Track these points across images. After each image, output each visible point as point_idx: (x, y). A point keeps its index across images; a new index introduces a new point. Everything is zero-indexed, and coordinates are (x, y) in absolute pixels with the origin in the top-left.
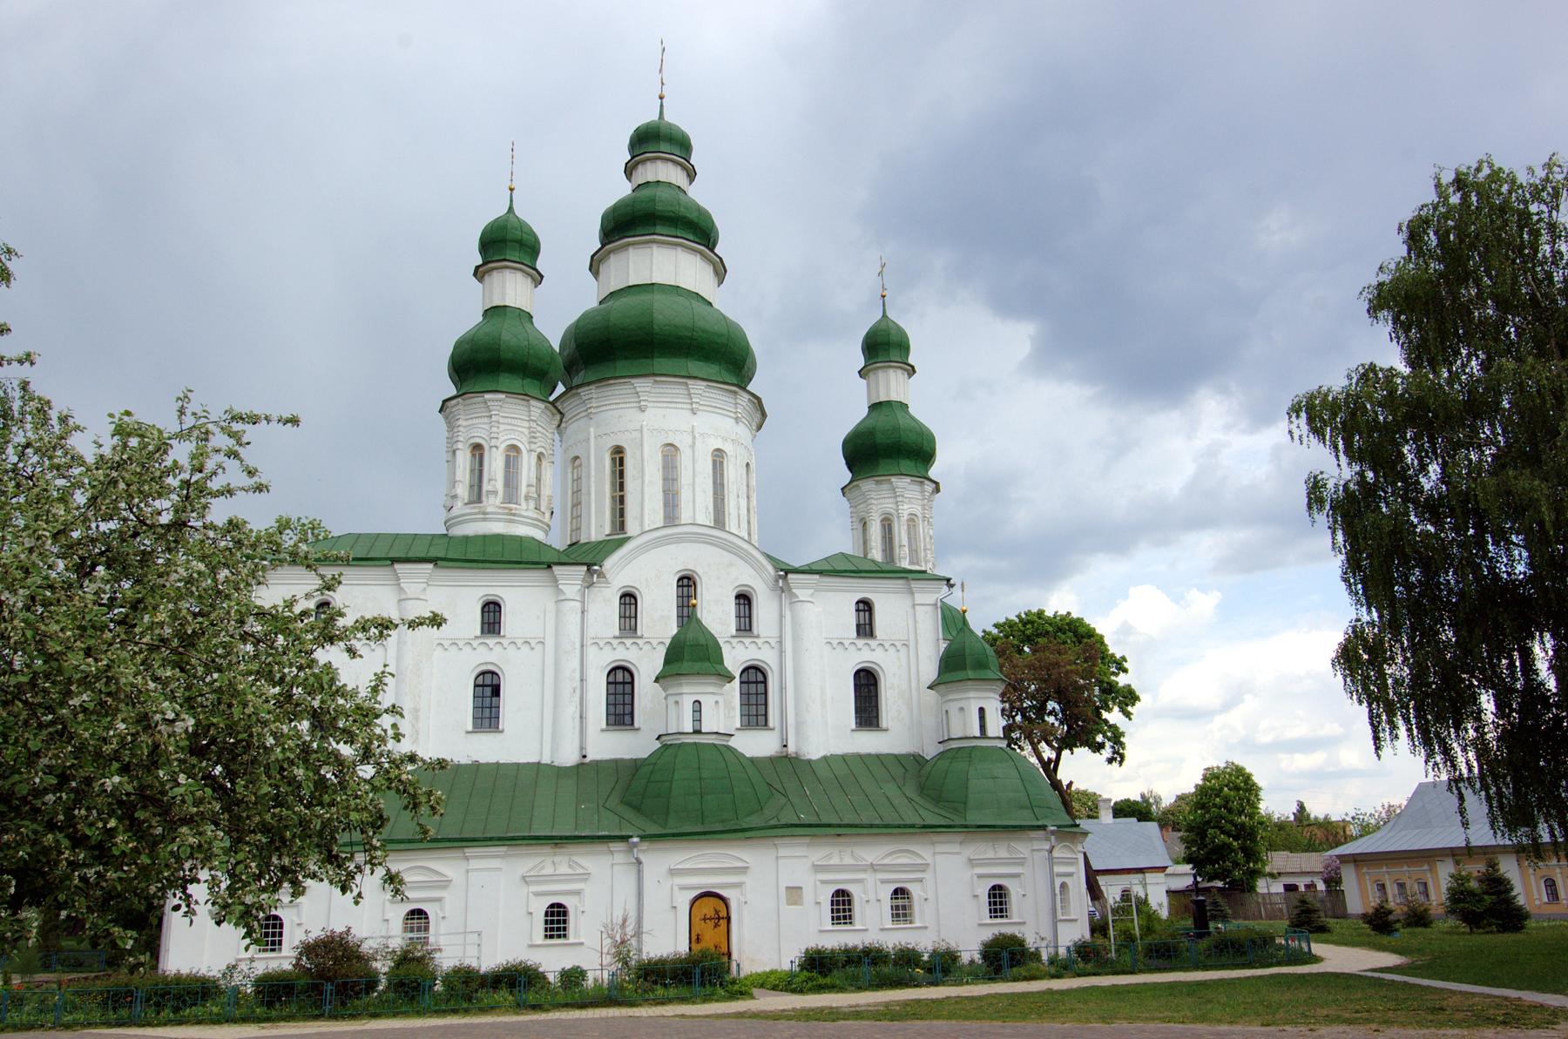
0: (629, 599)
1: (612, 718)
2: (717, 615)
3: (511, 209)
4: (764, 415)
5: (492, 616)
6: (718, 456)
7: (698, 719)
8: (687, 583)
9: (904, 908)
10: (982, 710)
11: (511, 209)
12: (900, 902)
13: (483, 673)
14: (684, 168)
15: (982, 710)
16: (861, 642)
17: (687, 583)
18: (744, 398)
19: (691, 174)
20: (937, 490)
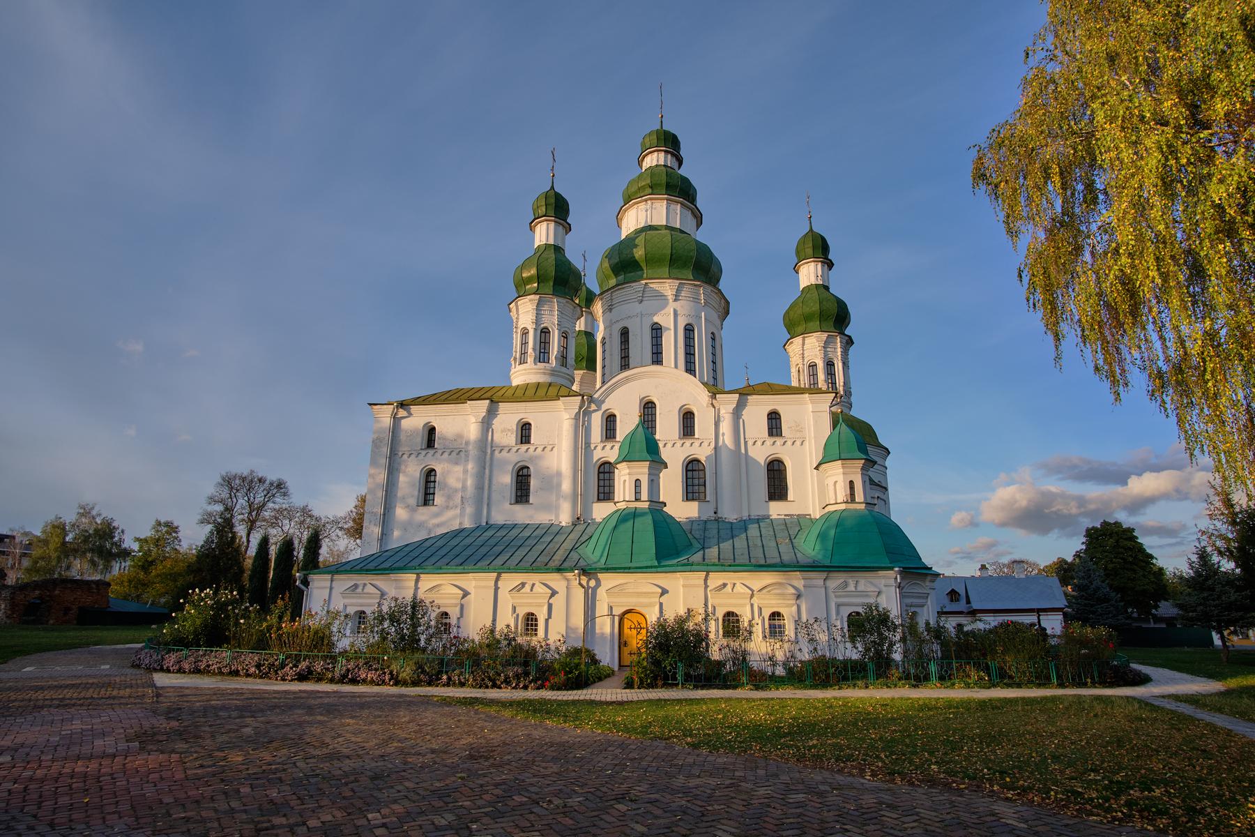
0: (610, 420)
1: (602, 496)
2: (667, 428)
3: (552, 187)
4: (728, 303)
5: (525, 432)
6: (689, 330)
7: (637, 492)
8: (648, 408)
9: (780, 626)
10: (851, 482)
11: (552, 187)
12: (777, 622)
13: (522, 468)
14: (673, 154)
15: (851, 482)
16: (769, 441)
17: (648, 408)
18: (709, 288)
19: (680, 162)
20: (852, 343)
